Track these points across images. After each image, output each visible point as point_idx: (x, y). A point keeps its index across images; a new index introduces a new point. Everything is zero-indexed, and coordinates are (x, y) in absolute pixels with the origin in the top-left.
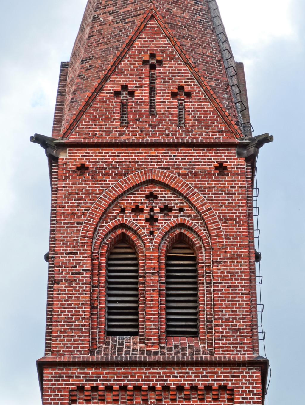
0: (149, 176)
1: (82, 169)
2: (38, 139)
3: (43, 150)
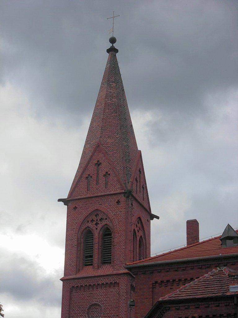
0: (96, 208)
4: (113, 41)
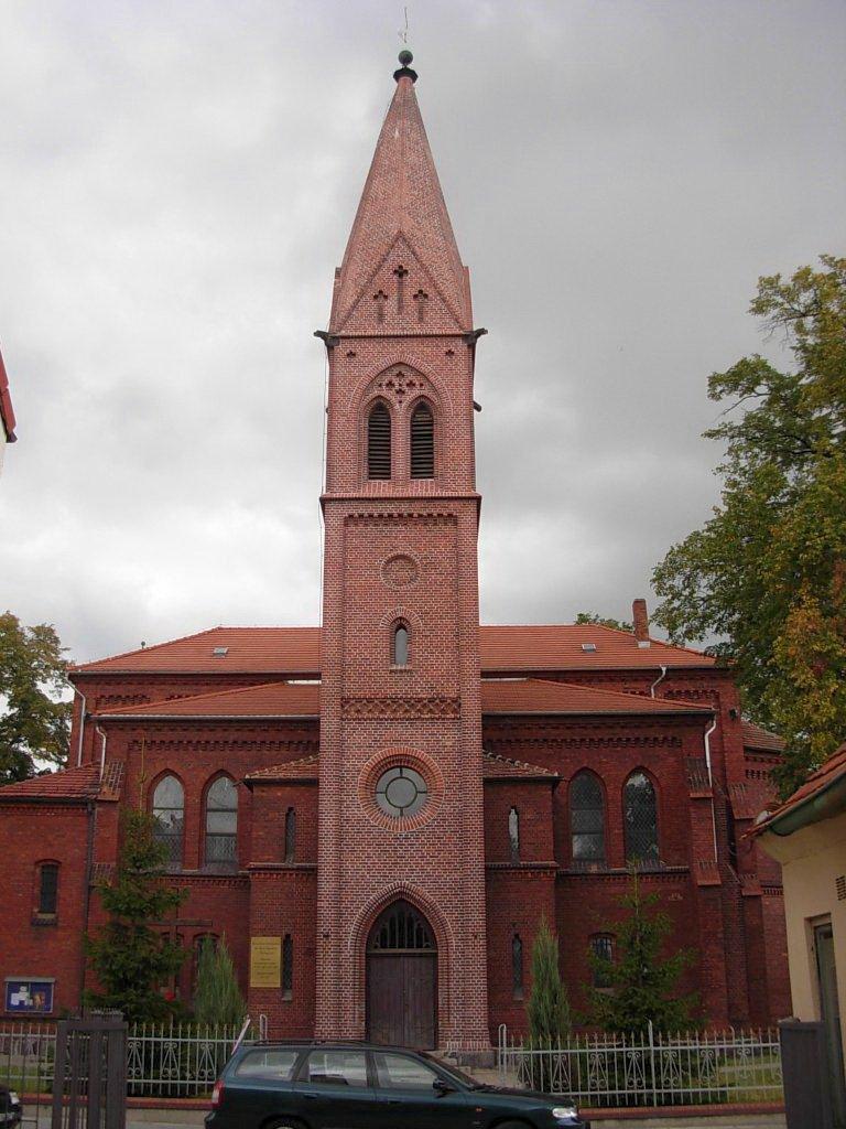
1: (352, 355)
2: (318, 334)
3: (323, 341)
4: (406, 58)
